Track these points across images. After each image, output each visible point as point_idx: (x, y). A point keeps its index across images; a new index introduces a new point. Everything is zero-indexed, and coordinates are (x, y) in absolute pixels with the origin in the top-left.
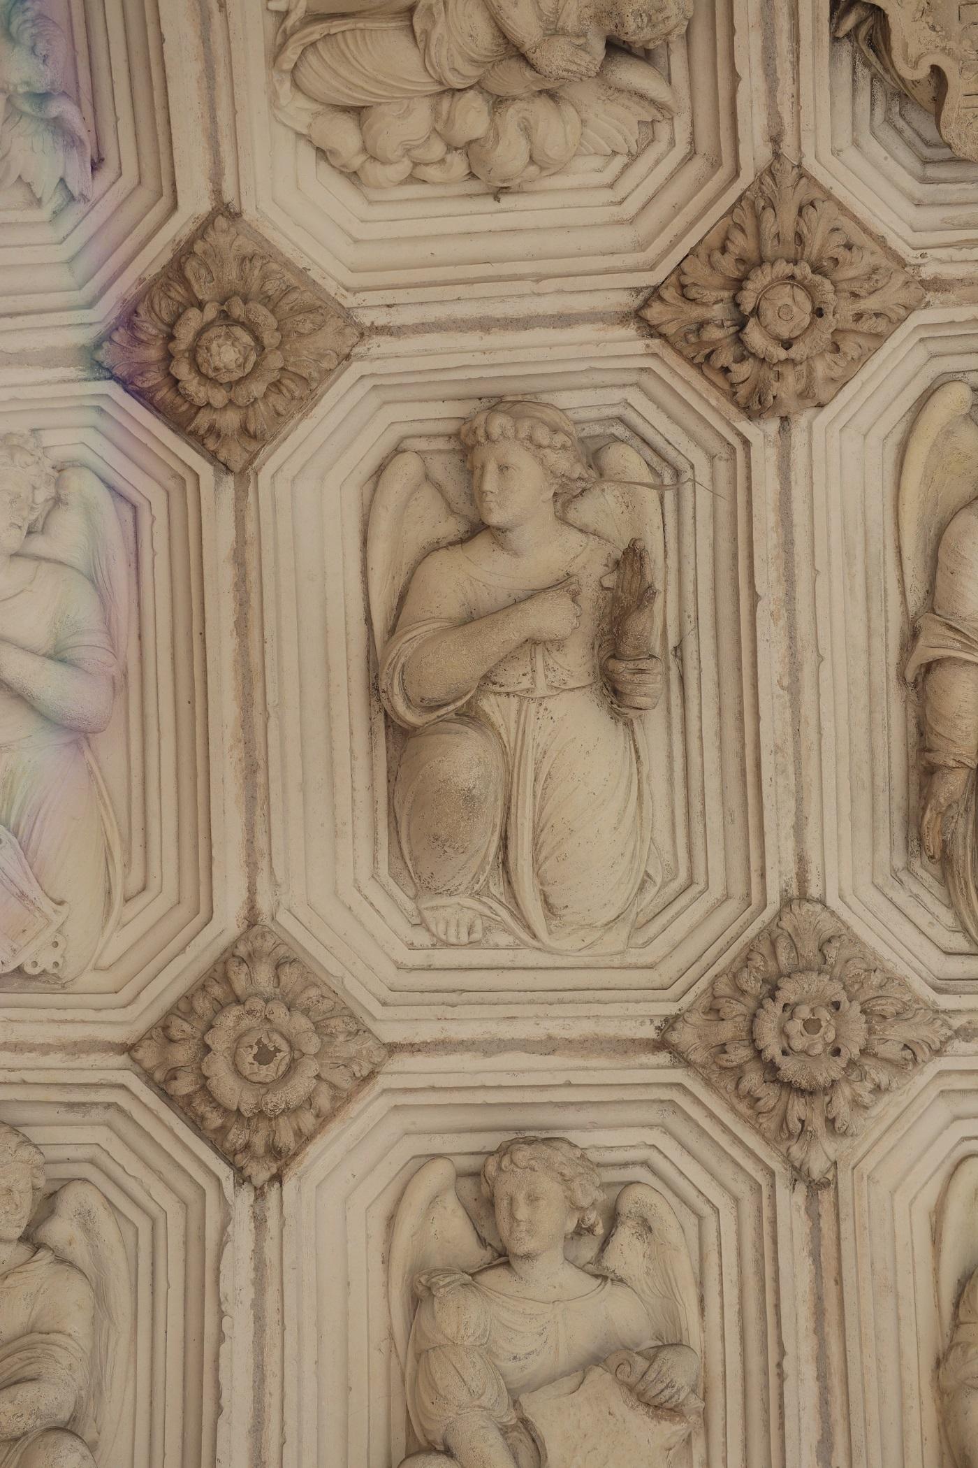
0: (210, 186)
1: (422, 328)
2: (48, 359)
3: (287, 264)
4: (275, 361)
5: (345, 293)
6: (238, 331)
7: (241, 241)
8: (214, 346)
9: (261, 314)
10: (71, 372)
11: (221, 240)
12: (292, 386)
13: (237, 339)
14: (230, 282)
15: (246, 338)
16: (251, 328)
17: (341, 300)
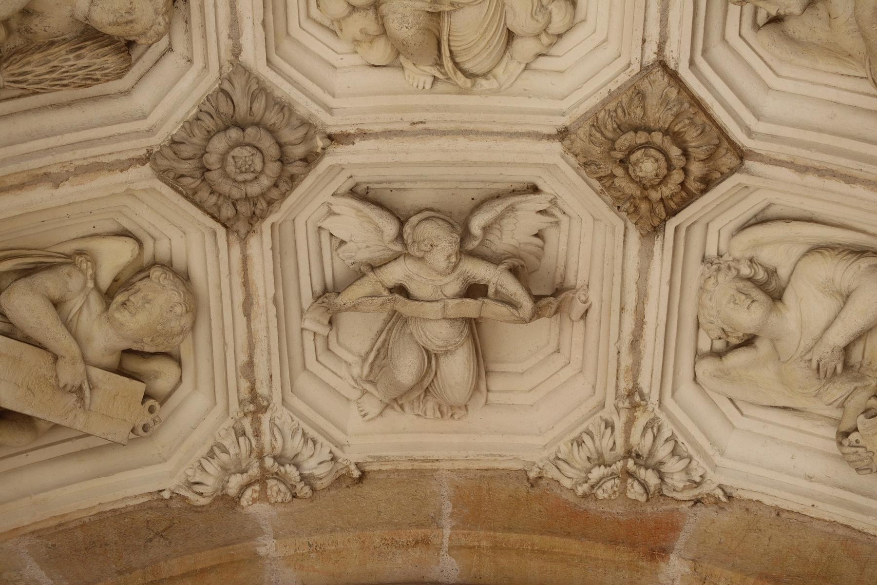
0: (544, 141)
1: (664, 21)
2: (647, 255)
3: (604, 103)
4: (657, 137)
5: (630, 69)
6: (633, 158)
7: (581, 132)
8: (641, 174)
9: (627, 140)
10: (658, 244)
11: (579, 145)
12: (680, 126)
13: (638, 160)
14: (602, 153)
15: (638, 154)
16: (631, 150)
17: (634, 73)
